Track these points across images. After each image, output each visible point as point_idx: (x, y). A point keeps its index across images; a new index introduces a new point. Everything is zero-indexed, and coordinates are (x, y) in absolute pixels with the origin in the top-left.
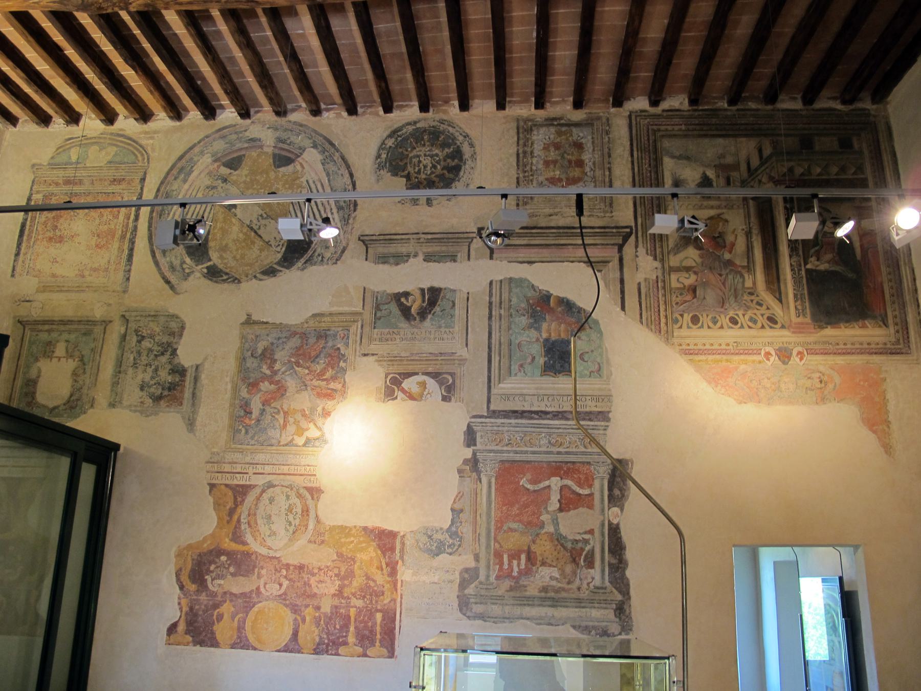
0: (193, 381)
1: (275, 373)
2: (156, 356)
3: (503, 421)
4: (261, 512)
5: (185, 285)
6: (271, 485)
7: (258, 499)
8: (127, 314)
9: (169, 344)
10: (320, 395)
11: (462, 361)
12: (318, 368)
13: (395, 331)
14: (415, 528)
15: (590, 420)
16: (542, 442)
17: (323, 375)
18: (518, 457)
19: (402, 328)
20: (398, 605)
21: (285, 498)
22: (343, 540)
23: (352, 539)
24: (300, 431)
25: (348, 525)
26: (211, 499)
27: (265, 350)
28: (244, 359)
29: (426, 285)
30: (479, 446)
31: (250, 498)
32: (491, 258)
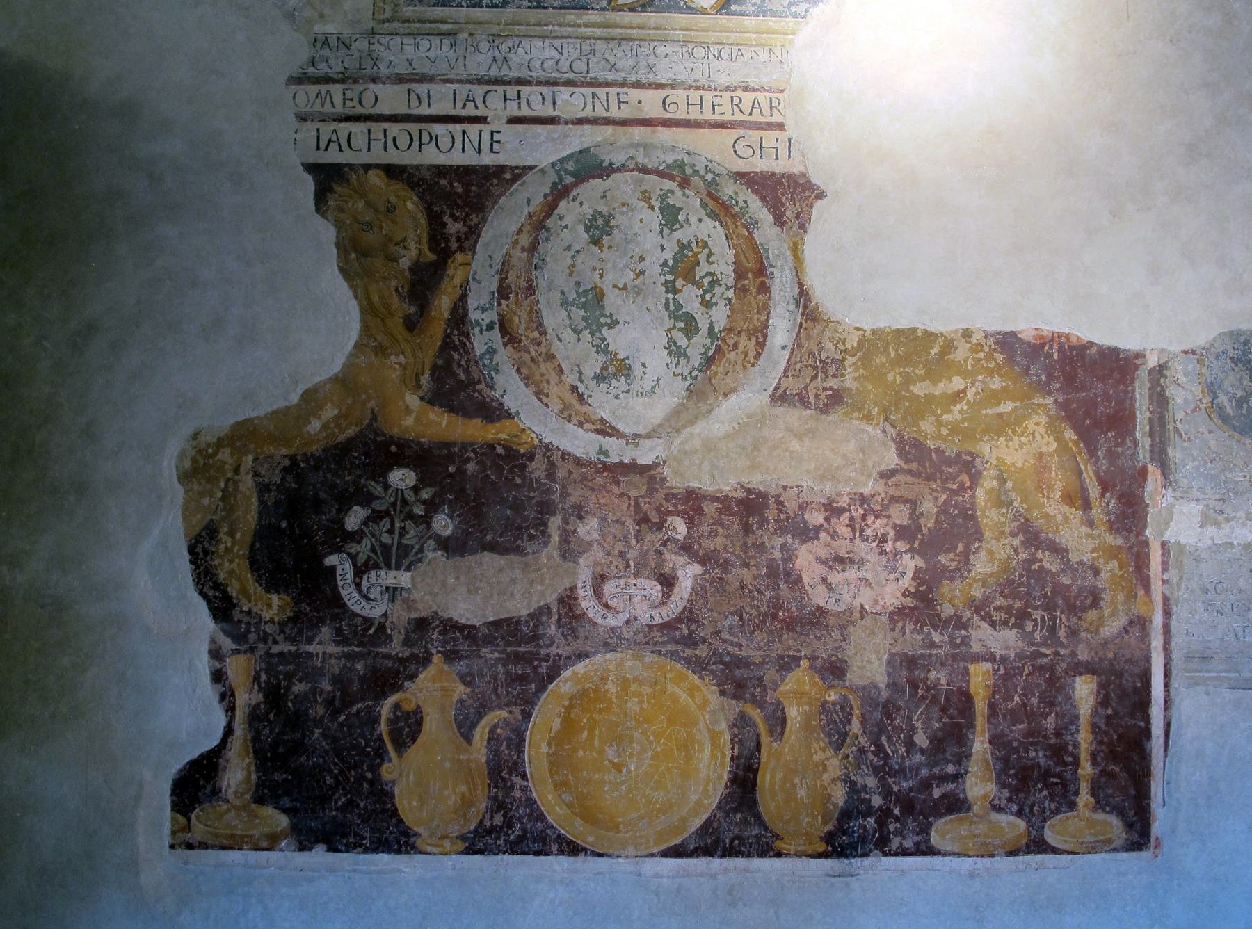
4: (555, 272)
6: (588, 168)
7: (539, 223)
14: (1201, 339)
20: (1157, 642)
21: (654, 219)
22: (919, 389)
23: (958, 383)
25: (935, 327)
26: (326, 232)
31: (503, 225)
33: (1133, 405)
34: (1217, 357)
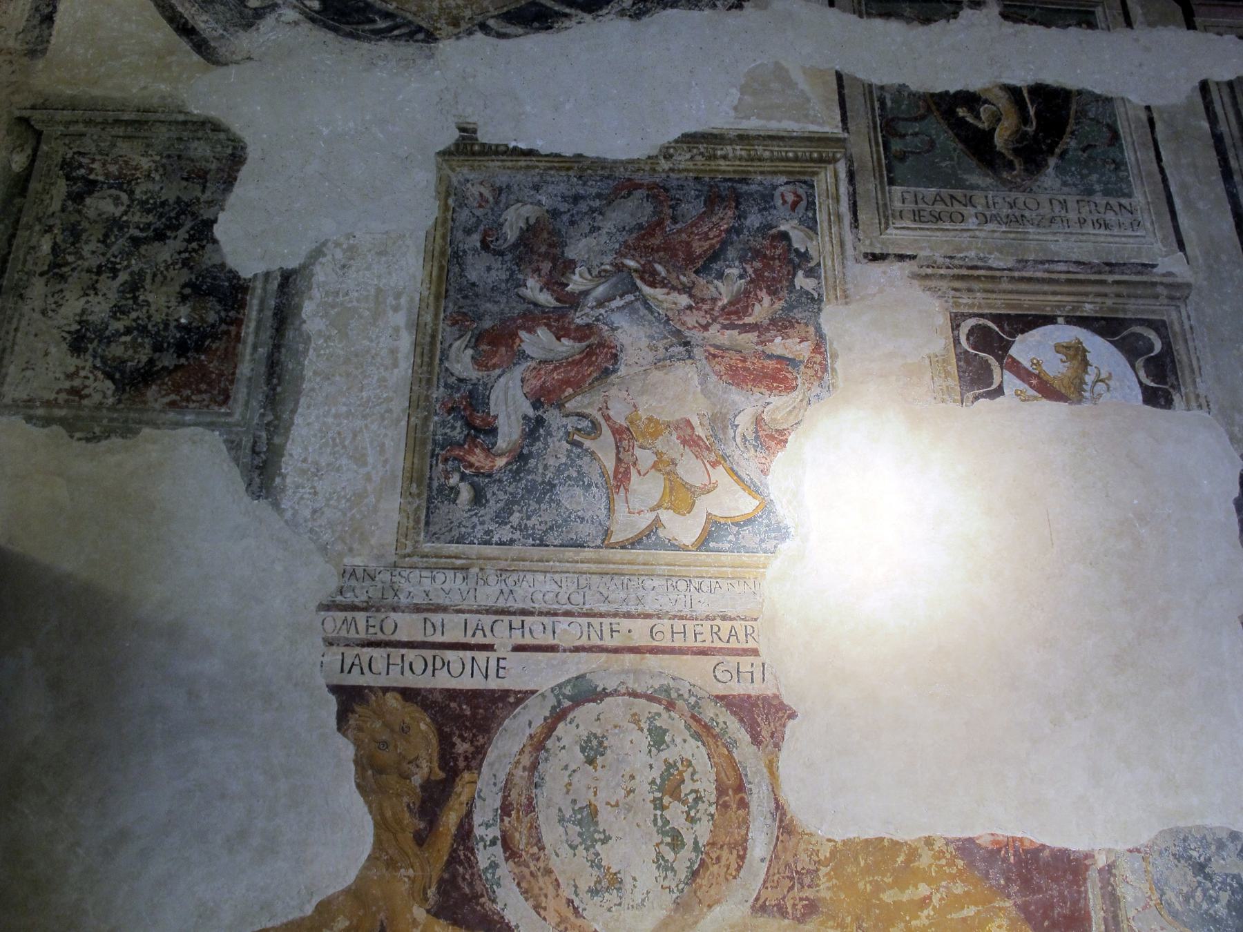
0: (269, 322)
1: (574, 301)
2: (136, 242)
4: (553, 795)
5: (245, 41)
6: (584, 693)
7: (539, 744)
8: (37, 115)
9: (185, 208)
10: (741, 376)
11: (1178, 292)
12: (725, 291)
13: (959, 193)
14: (1144, 838)
17: (745, 311)
19: (977, 187)
21: (644, 740)
22: (888, 897)
23: (923, 889)
24: (681, 496)
25: (899, 837)
26: (346, 750)
27: (530, 232)
28: (458, 257)
29: (1022, 77)
31: (508, 744)
32: (1191, 25)
33: (1087, 905)
34: (1161, 854)
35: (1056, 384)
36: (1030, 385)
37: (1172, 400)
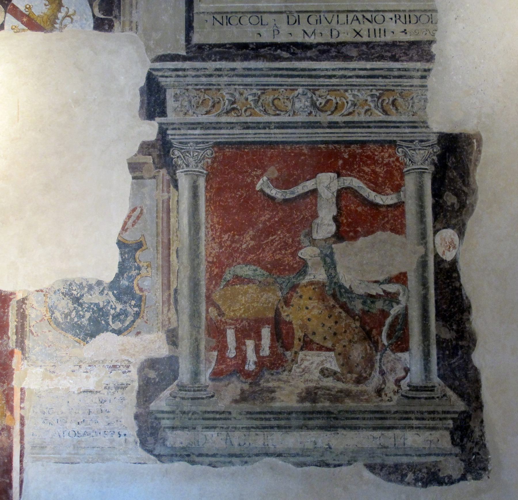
3: (218, 64)
14: (46, 284)
15: (394, 59)
16: (297, 105)
18: (250, 136)
20: (16, 439)
30: (172, 117)
33: (8, 319)
34: (55, 292)
35: (38, 22)
36: (23, 23)
37: (113, 26)
